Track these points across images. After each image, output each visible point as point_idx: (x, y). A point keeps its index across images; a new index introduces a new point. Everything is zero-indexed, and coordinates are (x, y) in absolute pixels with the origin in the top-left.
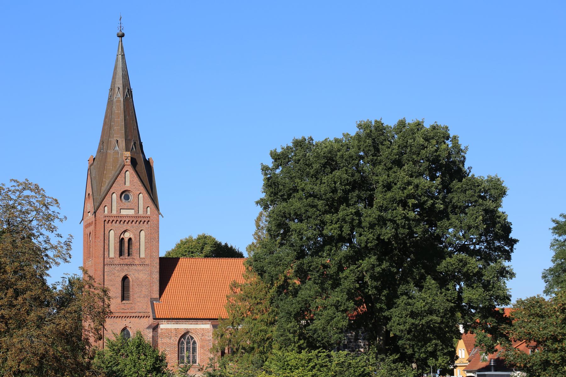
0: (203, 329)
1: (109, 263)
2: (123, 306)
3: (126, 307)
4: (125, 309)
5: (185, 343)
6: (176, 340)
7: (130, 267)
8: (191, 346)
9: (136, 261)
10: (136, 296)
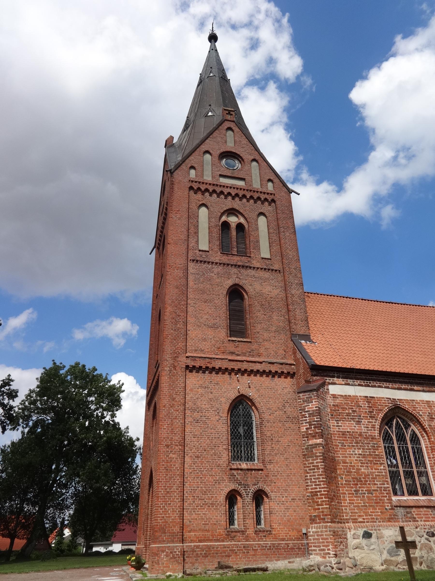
0: (428, 402)
1: (198, 259)
2: (231, 347)
3: (238, 349)
4: (237, 353)
5: (394, 438)
6: (373, 427)
7: (243, 271)
9: (254, 262)
10: (258, 327)
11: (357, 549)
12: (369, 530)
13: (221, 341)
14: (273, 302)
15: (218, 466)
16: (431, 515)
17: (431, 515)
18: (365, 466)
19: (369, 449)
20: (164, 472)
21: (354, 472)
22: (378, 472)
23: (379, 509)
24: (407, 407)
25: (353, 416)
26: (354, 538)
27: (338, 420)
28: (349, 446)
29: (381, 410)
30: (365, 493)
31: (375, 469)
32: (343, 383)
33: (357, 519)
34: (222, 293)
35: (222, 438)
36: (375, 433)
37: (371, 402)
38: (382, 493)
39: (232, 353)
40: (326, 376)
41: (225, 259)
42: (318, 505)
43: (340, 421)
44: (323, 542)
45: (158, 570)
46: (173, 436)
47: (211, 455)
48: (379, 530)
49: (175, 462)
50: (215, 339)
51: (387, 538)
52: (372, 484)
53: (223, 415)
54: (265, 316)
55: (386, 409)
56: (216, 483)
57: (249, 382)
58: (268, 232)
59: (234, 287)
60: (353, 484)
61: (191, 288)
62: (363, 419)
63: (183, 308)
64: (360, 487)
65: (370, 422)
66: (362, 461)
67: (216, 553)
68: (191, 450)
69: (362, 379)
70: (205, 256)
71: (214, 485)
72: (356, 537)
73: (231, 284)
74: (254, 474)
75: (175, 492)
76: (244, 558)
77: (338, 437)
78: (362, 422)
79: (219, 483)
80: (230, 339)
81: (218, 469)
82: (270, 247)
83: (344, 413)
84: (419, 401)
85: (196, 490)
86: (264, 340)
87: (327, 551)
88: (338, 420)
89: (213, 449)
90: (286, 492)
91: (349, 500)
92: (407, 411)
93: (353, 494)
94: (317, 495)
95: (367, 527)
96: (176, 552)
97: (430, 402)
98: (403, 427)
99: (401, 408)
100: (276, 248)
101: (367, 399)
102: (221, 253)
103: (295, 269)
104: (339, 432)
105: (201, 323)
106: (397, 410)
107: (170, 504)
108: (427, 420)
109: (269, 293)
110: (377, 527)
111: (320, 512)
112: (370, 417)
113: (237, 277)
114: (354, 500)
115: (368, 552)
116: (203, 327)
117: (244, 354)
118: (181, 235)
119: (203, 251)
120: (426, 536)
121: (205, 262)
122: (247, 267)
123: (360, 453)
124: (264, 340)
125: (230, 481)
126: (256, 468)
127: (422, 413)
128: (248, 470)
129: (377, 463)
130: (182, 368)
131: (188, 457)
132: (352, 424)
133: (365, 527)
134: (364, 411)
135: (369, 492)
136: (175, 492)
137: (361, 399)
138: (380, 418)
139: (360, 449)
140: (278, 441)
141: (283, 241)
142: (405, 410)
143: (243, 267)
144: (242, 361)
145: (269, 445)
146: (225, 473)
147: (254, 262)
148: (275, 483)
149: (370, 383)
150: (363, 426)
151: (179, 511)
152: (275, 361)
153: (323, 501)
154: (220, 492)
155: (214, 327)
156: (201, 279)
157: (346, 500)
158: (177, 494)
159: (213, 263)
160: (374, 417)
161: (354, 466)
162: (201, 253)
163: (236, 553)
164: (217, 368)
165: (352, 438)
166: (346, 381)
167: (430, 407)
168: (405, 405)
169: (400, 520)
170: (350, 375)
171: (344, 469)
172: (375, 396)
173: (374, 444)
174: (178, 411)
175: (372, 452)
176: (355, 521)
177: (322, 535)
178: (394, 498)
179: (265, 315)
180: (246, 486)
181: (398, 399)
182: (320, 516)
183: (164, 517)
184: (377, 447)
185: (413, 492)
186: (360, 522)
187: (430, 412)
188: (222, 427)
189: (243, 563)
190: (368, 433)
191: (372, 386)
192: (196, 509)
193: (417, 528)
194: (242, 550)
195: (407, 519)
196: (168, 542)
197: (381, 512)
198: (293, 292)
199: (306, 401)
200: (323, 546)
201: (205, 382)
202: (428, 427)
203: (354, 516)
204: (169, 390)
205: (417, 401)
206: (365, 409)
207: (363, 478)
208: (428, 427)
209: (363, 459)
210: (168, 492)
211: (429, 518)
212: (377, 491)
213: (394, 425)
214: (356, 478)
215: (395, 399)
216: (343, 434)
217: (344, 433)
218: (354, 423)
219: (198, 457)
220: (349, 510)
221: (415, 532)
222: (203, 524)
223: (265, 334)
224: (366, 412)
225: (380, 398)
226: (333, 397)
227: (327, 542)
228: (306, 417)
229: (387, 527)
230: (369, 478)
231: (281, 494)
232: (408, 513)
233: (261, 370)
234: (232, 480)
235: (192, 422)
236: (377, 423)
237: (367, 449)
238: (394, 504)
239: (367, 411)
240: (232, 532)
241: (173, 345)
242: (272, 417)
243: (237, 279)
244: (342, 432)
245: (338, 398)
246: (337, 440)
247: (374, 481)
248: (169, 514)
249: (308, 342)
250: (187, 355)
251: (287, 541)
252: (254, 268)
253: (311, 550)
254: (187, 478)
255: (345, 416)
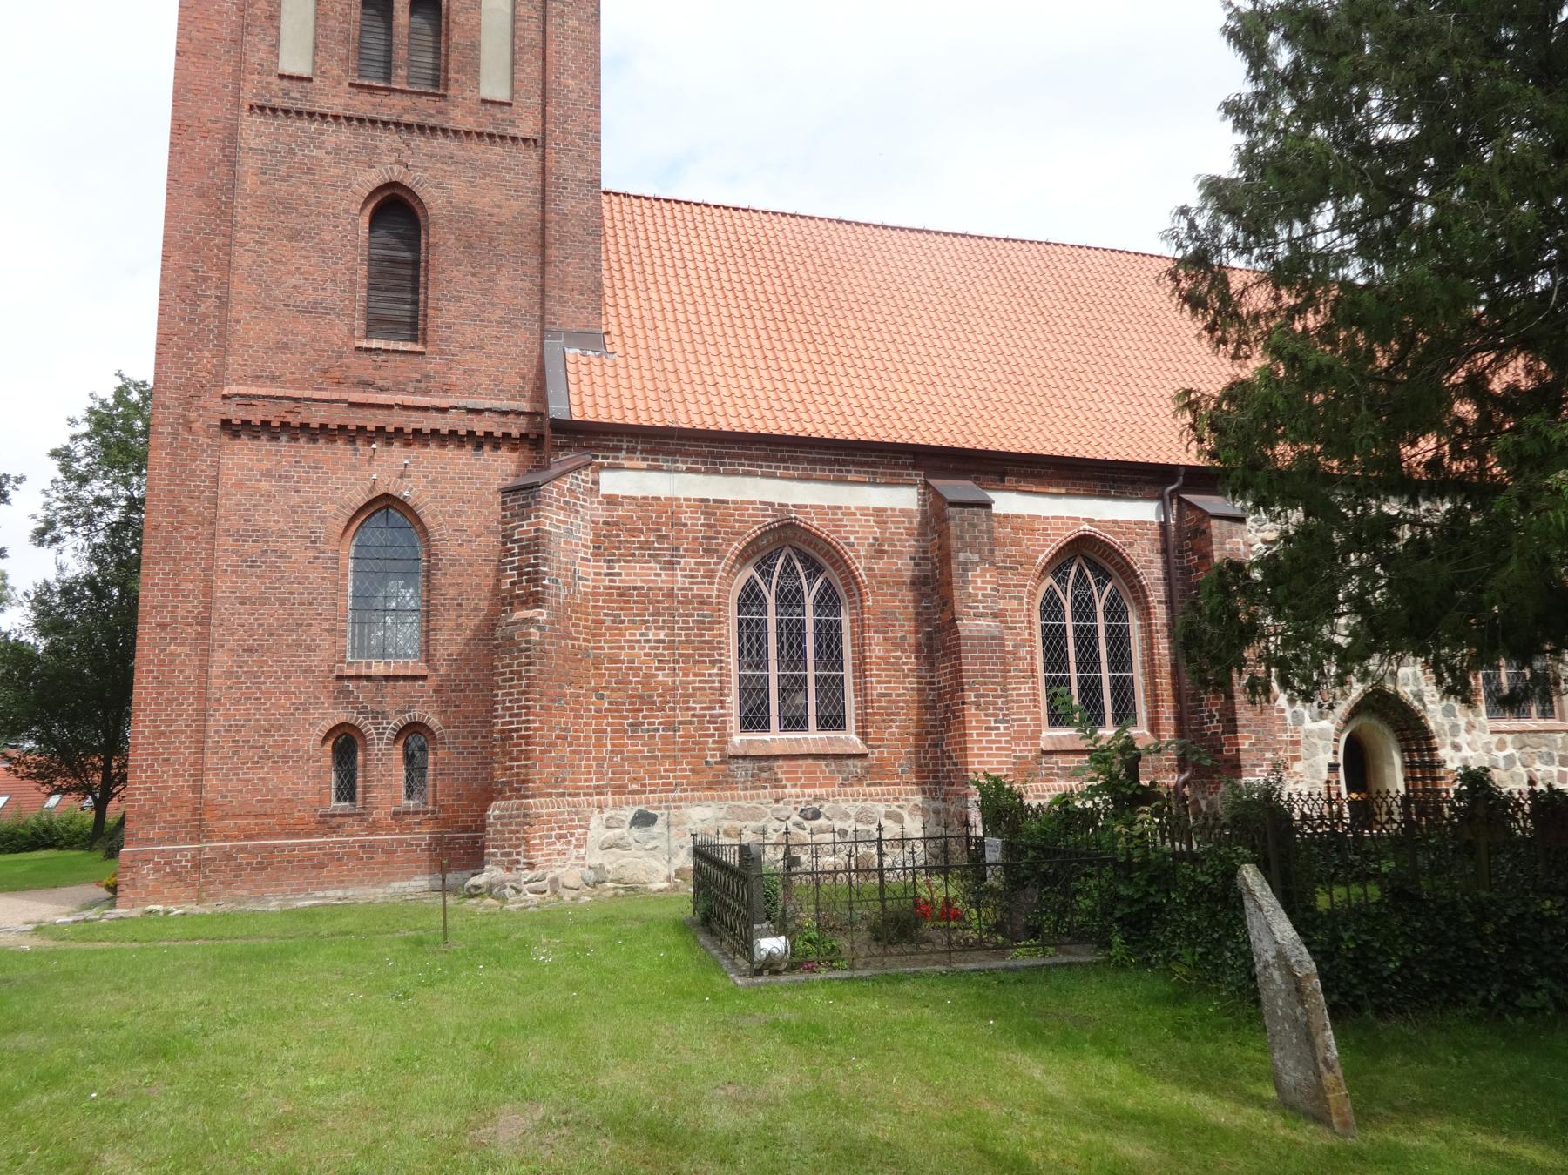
0: (879, 512)
1: (277, 103)
2: (363, 367)
3: (383, 373)
4: (380, 383)
5: (771, 600)
6: (710, 575)
7: (418, 140)
8: (810, 619)
9: (457, 113)
11: (613, 850)
12: (652, 808)
13: (333, 351)
14: (502, 237)
15: (306, 671)
16: (824, 772)
17: (824, 772)
18: (669, 668)
19: (688, 629)
20: (153, 688)
21: (638, 682)
22: (700, 682)
23: (688, 764)
24: (815, 523)
25: (655, 549)
26: (608, 827)
27: (612, 561)
28: (633, 622)
29: (740, 533)
30: (658, 730)
31: (695, 675)
32: (644, 465)
33: (626, 786)
34: (347, 211)
35: (320, 604)
36: (712, 590)
37: (715, 514)
38: (701, 729)
39: (366, 384)
40: (596, 448)
41: (363, 105)
42: (512, 760)
43: (619, 561)
44: (511, 839)
45: (134, 900)
46: (181, 602)
47: (288, 645)
48: (678, 808)
49: (183, 663)
50: (316, 346)
51: (695, 823)
52: (680, 709)
53: (328, 548)
54: (473, 279)
55: (754, 531)
56: (298, 709)
57: (406, 461)
58: (514, 15)
59: (387, 193)
60: (627, 710)
61: (250, 196)
62: (684, 556)
63: (217, 256)
64: (645, 717)
65: (704, 564)
66: (664, 655)
67: (289, 862)
68: (233, 634)
69: (699, 455)
70: (297, 95)
71: (292, 714)
72: (615, 824)
73: (377, 183)
74: (401, 686)
75: (182, 732)
76: (359, 870)
77: (604, 601)
78: (679, 563)
79: (306, 709)
80: (364, 344)
81: (305, 678)
82: (514, 63)
83: (633, 542)
84: (853, 510)
85: (243, 726)
86: (464, 348)
87: (515, 857)
88: (612, 561)
89: (293, 631)
90: (483, 727)
91: (613, 745)
92: (814, 534)
93: (625, 731)
94: (512, 738)
95: (647, 802)
96: (180, 861)
97: (885, 510)
98: (802, 575)
99: (799, 526)
100: (531, 69)
101: (706, 507)
102: (351, 85)
103: (582, 136)
104: (611, 588)
105: (275, 299)
106: (789, 532)
107: (168, 760)
108: (865, 557)
109: (496, 211)
110: (674, 801)
111: (513, 775)
112: (704, 550)
113: (398, 162)
114: (625, 745)
115: (641, 853)
116: (281, 311)
117: (400, 387)
118: (220, 23)
119: (291, 78)
120: (796, 818)
121: (299, 113)
122: (433, 129)
123: (662, 637)
124: (464, 348)
125: (335, 706)
126: (410, 673)
127: (856, 538)
128: (387, 678)
129: (705, 662)
130: (210, 426)
131: (224, 652)
132: (651, 568)
133: (640, 803)
134: (690, 535)
135: (670, 726)
136: (182, 732)
137: (687, 507)
138: (733, 553)
139: (662, 628)
140: (475, 610)
141: (552, 47)
142: (809, 531)
143: (421, 128)
144: (389, 407)
145: (449, 620)
146: (325, 687)
147: (457, 113)
148: (456, 706)
149: (722, 464)
150: (679, 573)
151: (190, 775)
152: (488, 404)
153: (521, 751)
154: (307, 730)
155: (315, 311)
156: (284, 168)
157: (605, 745)
158: (187, 737)
159: (323, 116)
160: (717, 551)
161: (640, 669)
162: (286, 83)
163: (340, 859)
164: (315, 425)
165: (644, 603)
166: (653, 460)
167: (881, 523)
168: (812, 519)
169: (740, 785)
170: (668, 444)
171: (610, 676)
172: (729, 497)
173: (704, 616)
174: (193, 538)
175: (695, 635)
176: (620, 790)
177: (510, 824)
178: (739, 740)
179: (474, 275)
180: (378, 716)
181: (794, 506)
182: (512, 782)
183: (150, 789)
184: (709, 622)
185: (795, 722)
186: (632, 793)
187: (878, 535)
188: (323, 578)
189: (356, 880)
190: (692, 589)
191: (726, 473)
192: (240, 769)
193: (777, 801)
194: (355, 853)
195: (758, 783)
196: (161, 841)
197: (692, 770)
198: (567, 206)
199: (517, 515)
200: (510, 846)
201: (279, 463)
202: (863, 573)
203: (620, 779)
204: (169, 485)
205: (849, 508)
206: (696, 532)
207: (659, 696)
208: (863, 573)
209: (666, 652)
210: (163, 733)
211: (818, 779)
212: (691, 723)
213: (778, 568)
214: (641, 697)
215: (787, 505)
216: (620, 595)
217: (623, 593)
218: (658, 566)
219: (250, 650)
220: (609, 766)
221: (769, 811)
222: (258, 801)
223: (468, 331)
224: (697, 538)
225: (742, 502)
226: (608, 503)
227: (517, 839)
228: (513, 555)
229: (701, 801)
230: (674, 696)
231: (470, 732)
232: (761, 770)
233: (445, 431)
234: (342, 703)
235: (238, 566)
236: (722, 565)
237: (681, 629)
238: (731, 751)
239: (700, 535)
240: (334, 816)
241: (185, 363)
242: (465, 550)
243: (396, 168)
244: (619, 588)
245: (622, 504)
246: (604, 608)
247: (688, 702)
248: (164, 781)
249: (590, 353)
250: (225, 392)
251: (476, 831)
252: (456, 132)
253: (488, 854)
254: (219, 699)
255: (635, 548)
